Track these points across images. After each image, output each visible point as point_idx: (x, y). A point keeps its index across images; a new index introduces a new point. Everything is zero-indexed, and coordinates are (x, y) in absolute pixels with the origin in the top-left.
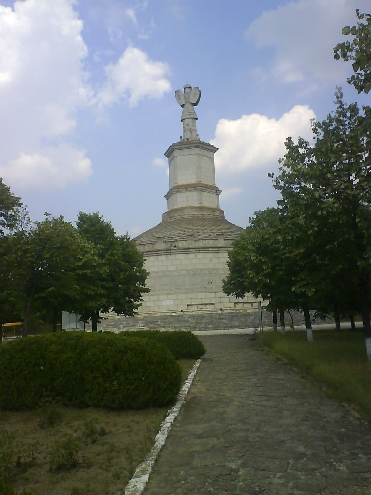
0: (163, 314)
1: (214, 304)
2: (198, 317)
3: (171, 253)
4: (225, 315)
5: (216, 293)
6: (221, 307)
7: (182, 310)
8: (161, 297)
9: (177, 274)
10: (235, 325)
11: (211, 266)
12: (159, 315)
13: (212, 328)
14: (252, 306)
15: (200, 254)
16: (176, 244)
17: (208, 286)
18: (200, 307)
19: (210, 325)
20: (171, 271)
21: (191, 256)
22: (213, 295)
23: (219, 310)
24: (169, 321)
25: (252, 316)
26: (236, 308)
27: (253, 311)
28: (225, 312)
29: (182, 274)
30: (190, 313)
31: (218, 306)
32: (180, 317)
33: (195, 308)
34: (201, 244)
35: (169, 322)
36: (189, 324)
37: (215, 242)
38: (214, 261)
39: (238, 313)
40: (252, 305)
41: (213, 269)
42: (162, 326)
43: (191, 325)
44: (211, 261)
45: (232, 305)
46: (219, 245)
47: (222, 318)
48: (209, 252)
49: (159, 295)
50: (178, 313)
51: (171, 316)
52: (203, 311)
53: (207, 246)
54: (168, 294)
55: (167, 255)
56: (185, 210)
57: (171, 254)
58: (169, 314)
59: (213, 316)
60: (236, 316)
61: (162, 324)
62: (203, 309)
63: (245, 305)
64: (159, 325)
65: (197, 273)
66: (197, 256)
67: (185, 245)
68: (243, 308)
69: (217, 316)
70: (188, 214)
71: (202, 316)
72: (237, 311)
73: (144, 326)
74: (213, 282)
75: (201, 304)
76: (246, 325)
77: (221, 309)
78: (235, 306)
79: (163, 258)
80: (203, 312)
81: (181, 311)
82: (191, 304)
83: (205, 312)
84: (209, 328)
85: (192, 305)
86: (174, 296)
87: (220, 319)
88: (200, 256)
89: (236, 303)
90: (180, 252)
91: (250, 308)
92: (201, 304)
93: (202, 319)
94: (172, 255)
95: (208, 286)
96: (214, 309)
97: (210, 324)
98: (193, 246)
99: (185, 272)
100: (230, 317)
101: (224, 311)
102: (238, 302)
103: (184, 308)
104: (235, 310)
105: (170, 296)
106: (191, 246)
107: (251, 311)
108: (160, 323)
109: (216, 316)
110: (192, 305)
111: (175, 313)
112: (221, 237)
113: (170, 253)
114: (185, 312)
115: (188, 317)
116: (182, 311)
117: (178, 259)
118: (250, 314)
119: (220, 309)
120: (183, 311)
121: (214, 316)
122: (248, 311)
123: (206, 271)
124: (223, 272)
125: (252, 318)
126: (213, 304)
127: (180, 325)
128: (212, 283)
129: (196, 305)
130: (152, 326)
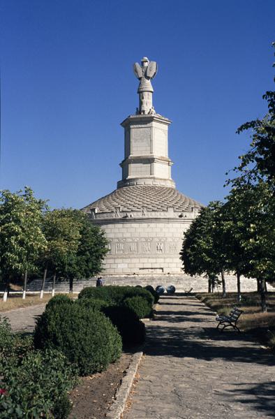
0: (117, 276)
8: (117, 261)
16: (132, 214)
18: (150, 270)
21: (144, 225)
22: (162, 260)
28: (172, 275)
31: (166, 271)
33: (145, 271)
34: (154, 215)
46: (168, 217)
53: (159, 217)
54: (123, 258)
67: (140, 215)
79: (120, 226)
85: (143, 269)
86: (128, 261)
88: (152, 225)
98: (146, 217)
103: (136, 271)
106: (144, 217)
110: (143, 269)
126: (162, 269)
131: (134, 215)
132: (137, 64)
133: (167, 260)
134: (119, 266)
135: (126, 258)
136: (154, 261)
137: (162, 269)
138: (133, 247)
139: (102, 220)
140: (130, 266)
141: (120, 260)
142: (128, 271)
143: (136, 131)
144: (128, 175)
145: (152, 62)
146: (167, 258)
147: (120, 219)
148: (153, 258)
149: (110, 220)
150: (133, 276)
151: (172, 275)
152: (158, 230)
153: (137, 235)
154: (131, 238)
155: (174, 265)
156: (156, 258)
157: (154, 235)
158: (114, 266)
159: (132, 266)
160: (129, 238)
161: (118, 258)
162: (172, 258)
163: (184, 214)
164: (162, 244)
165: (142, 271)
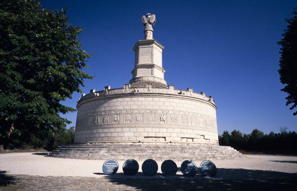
0: (124, 144)
8: (124, 130)
12: (122, 144)
21: (150, 99)
28: (173, 144)
29: (141, 112)
30: (146, 144)
31: (168, 140)
37: (168, 90)
49: (122, 127)
51: (131, 145)
53: (162, 93)
54: (130, 127)
58: (129, 144)
67: (145, 91)
71: (158, 148)
73: (107, 153)
75: (155, 137)
77: (171, 142)
79: (128, 99)
85: (148, 137)
86: (134, 130)
88: (156, 99)
92: (155, 137)
95: (161, 123)
98: (151, 92)
103: (142, 139)
105: (131, 129)
106: (149, 92)
110: (148, 137)
126: (165, 138)
129: (152, 137)
131: (141, 90)
132: (144, 16)
133: (170, 130)
134: (126, 134)
135: (132, 127)
137: (165, 138)
138: (140, 117)
139: (113, 95)
140: (136, 135)
141: (126, 129)
142: (134, 139)
143: (142, 50)
144: (138, 63)
145: (153, 15)
147: (129, 94)
148: (157, 128)
149: (120, 94)
150: (138, 144)
152: (161, 104)
153: (143, 107)
156: (159, 127)
157: (157, 108)
158: (122, 134)
159: (138, 134)
160: (136, 110)
161: (125, 127)
164: (165, 116)
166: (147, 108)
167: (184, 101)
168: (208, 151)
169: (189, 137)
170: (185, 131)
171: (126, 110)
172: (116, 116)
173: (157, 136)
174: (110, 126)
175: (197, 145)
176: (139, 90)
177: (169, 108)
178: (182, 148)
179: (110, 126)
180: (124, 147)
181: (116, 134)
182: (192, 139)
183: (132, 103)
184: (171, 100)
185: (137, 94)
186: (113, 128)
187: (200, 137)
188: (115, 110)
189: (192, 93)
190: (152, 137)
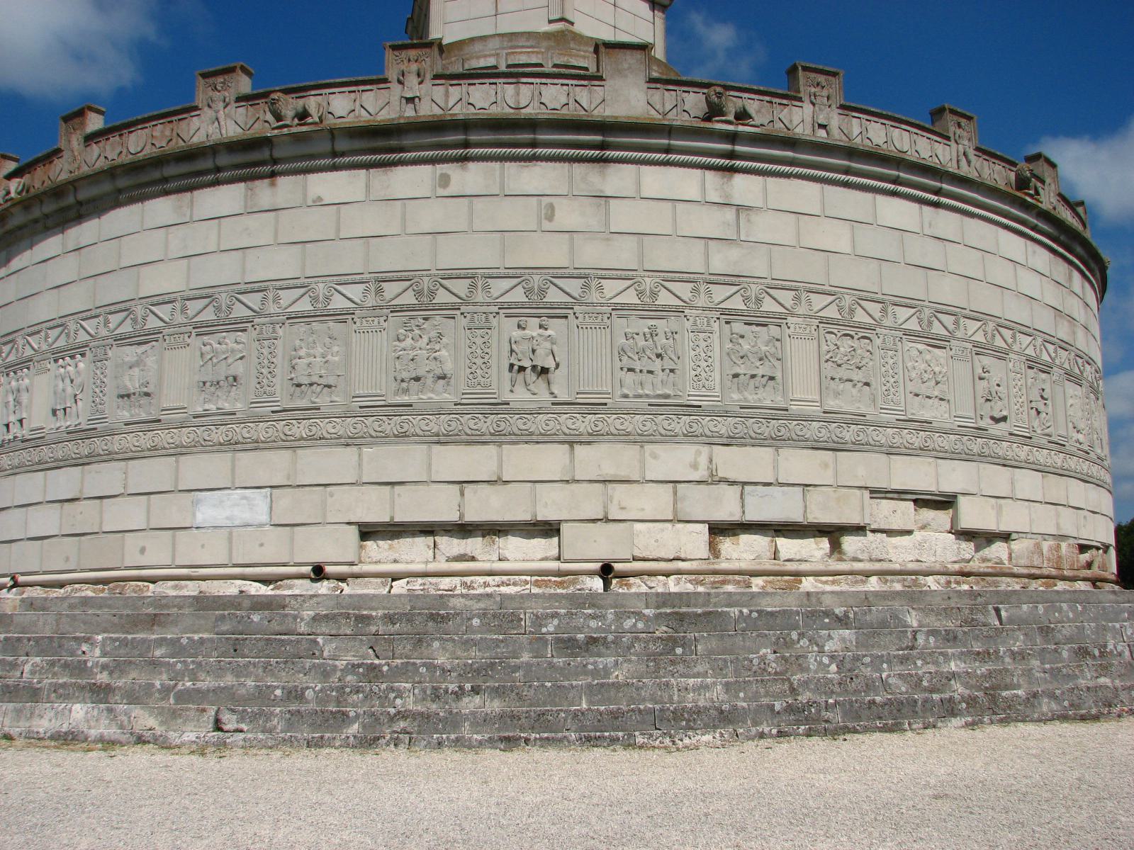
1: (558, 531)
2: (390, 619)
3: (278, 167)
4: (619, 617)
5: (571, 444)
6: (606, 554)
7: (317, 558)
8: (197, 469)
9: (305, 306)
10: (690, 700)
11: (553, 254)
13: (481, 721)
14: (836, 547)
15: (471, 165)
16: (312, 103)
17: (520, 396)
19: (477, 699)
20: (259, 288)
22: (550, 460)
23: (591, 573)
24: (161, 642)
25: (843, 622)
26: (724, 566)
27: (844, 586)
29: (338, 303)
32: (256, 618)
33: (414, 552)
35: (158, 653)
36: (301, 680)
37: (583, 95)
38: (569, 215)
39: (731, 600)
40: (836, 547)
41: (556, 274)
42: (103, 678)
43: (313, 687)
44: (550, 218)
45: (694, 541)
47: (592, 641)
48: (535, 158)
49: (180, 451)
50: (290, 587)
52: (468, 579)
54: (232, 445)
55: (250, 184)
56: (478, 47)
57: (273, 175)
59: (515, 619)
60: (711, 620)
61: (104, 667)
62: (473, 559)
63: (789, 547)
64: (80, 668)
65: (442, 297)
66: (445, 180)
68: (769, 565)
69: (547, 616)
70: (491, 62)
72: (730, 588)
74: (557, 366)
75: (464, 530)
76: (790, 709)
78: (714, 549)
80: (470, 587)
81: (307, 570)
82: (387, 519)
83: (486, 585)
84: (453, 721)
85: (394, 530)
86: (274, 465)
87: (568, 645)
88: (471, 177)
89: (719, 530)
90: (335, 154)
91: (821, 567)
92: (464, 530)
93: (420, 641)
94: (281, 181)
95: (520, 396)
96: (554, 565)
97: (476, 690)
98: (427, 110)
99: (355, 292)
100: (662, 630)
101: (632, 580)
102: (736, 517)
104: (712, 578)
105: (245, 458)
107: (828, 588)
108: (98, 652)
109: (539, 620)
110: (394, 530)
111: (271, 587)
112: (631, 59)
113: (267, 169)
114: (342, 578)
115: (314, 619)
116: (319, 573)
117: (319, 203)
118: (827, 614)
119: (597, 566)
120: (329, 569)
121: (527, 622)
122: (808, 584)
123: (507, 284)
124: (631, 298)
125: (836, 641)
126: (549, 529)
127: (229, 680)
128: (545, 371)
129: (428, 530)
130: (33, 672)
133: (594, 460)
134: (210, 511)
135: (257, 446)
136: (479, 461)
146: (591, 439)
151: (638, 586)
153: (350, 260)
154: (302, 285)
155: (655, 501)
156: (498, 438)
157: (481, 255)
162: (640, 440)
163: (733, 104)
165: (380, 553)
166: (389, 259)
167: (745, 187)
168: (951, 638)
169: (795, 516)
170: (733, 462)
171: (207, 295)
172: (130, 353)
173: (470, 517)
174: (99, 445)
175: (874, 584)
176: (313, 110)
177: (592, 255)
178: (681, 617)
179: (99, 445)
180: (135, 622)
181: (128, 514)
182: (833, 533)
183: (259, 229)
184: (618, 178)
185: (298, 138)
186: (110, 457)
187: (903, 513)
188: (124, 307)
189: (835, 119)
190: (428, 530)
